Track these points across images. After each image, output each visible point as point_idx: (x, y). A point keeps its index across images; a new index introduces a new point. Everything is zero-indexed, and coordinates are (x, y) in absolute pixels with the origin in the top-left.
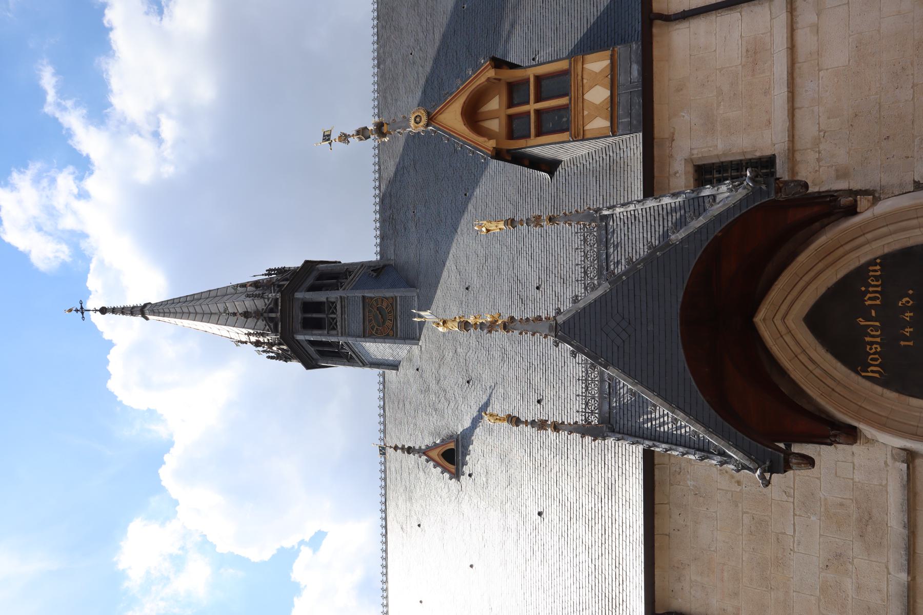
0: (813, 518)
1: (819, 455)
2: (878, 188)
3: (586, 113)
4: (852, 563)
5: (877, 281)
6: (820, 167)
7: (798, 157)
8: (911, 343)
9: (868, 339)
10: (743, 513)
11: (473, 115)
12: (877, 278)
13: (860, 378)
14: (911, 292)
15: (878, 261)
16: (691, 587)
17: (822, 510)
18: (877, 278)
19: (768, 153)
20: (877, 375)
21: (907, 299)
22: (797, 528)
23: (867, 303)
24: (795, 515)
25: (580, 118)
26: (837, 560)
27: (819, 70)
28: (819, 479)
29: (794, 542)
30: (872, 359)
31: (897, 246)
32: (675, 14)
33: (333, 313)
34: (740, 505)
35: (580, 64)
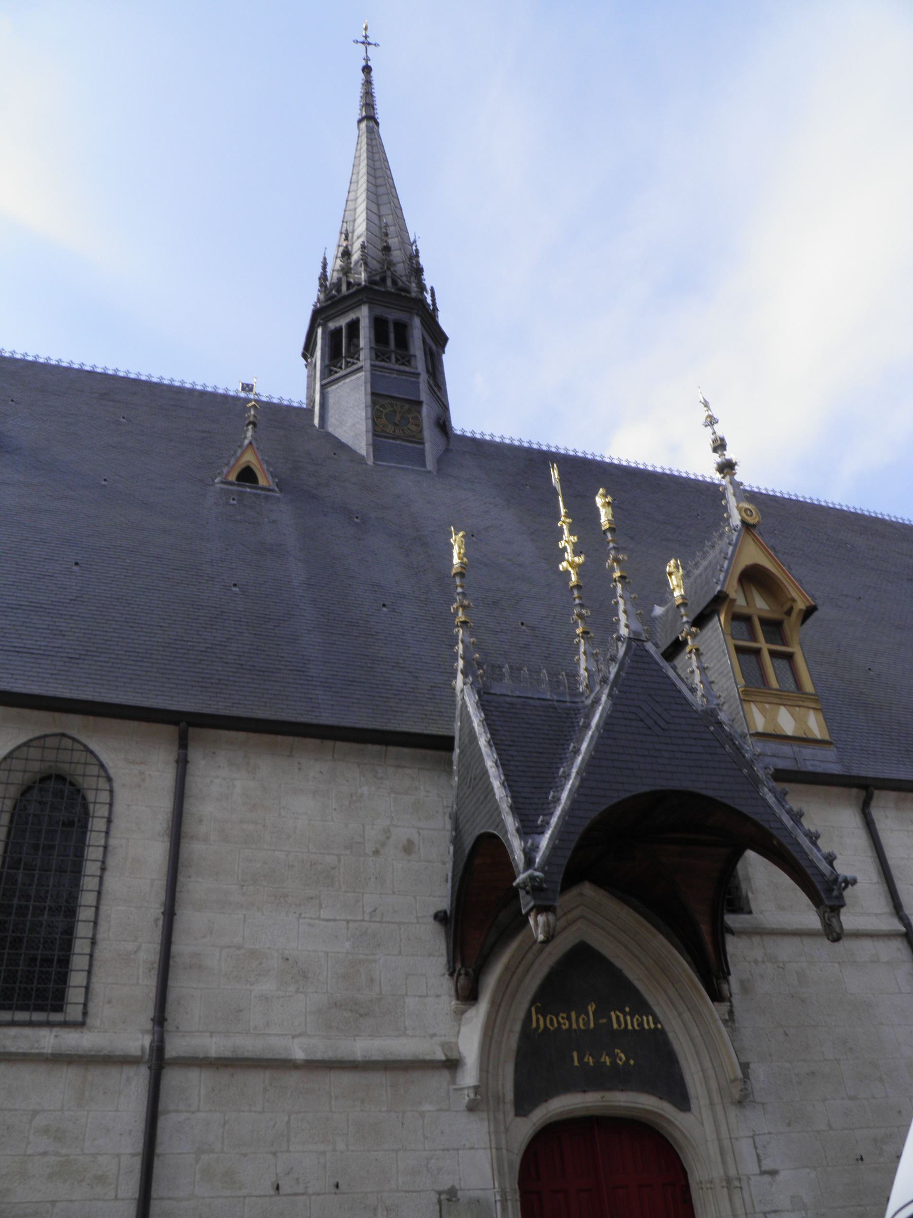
0: (348, 945)
1: (430, 955)
2: (737, 1025)
3: (767, 706)
4: (297, 991)
5: (638, 1025)
6: (749, 963)
7: (756, 939)
8: (576, 1063)
9: (573, 1014)
10: (338, 856)
11: (753, 577)
12: (641, 1024)
13: (525, 1005)
15: (659, 1026)
16: (224, 779)
17: (361, 957)
18: (641, 1024)
19: (753, 906)
20: (534, 1025)
22: (330, 923)
23: (612, 1014)
24: (348, 922)
25: (762, 699)
26: (298, 973)
27: (839, 963)
28: (400, 953)
29: (311, 918)
30: (551, 1020)
31: (676, 1046)
32: (870, 814)
33: (397, 360)
34: (348, 852)
35: (813, 705)
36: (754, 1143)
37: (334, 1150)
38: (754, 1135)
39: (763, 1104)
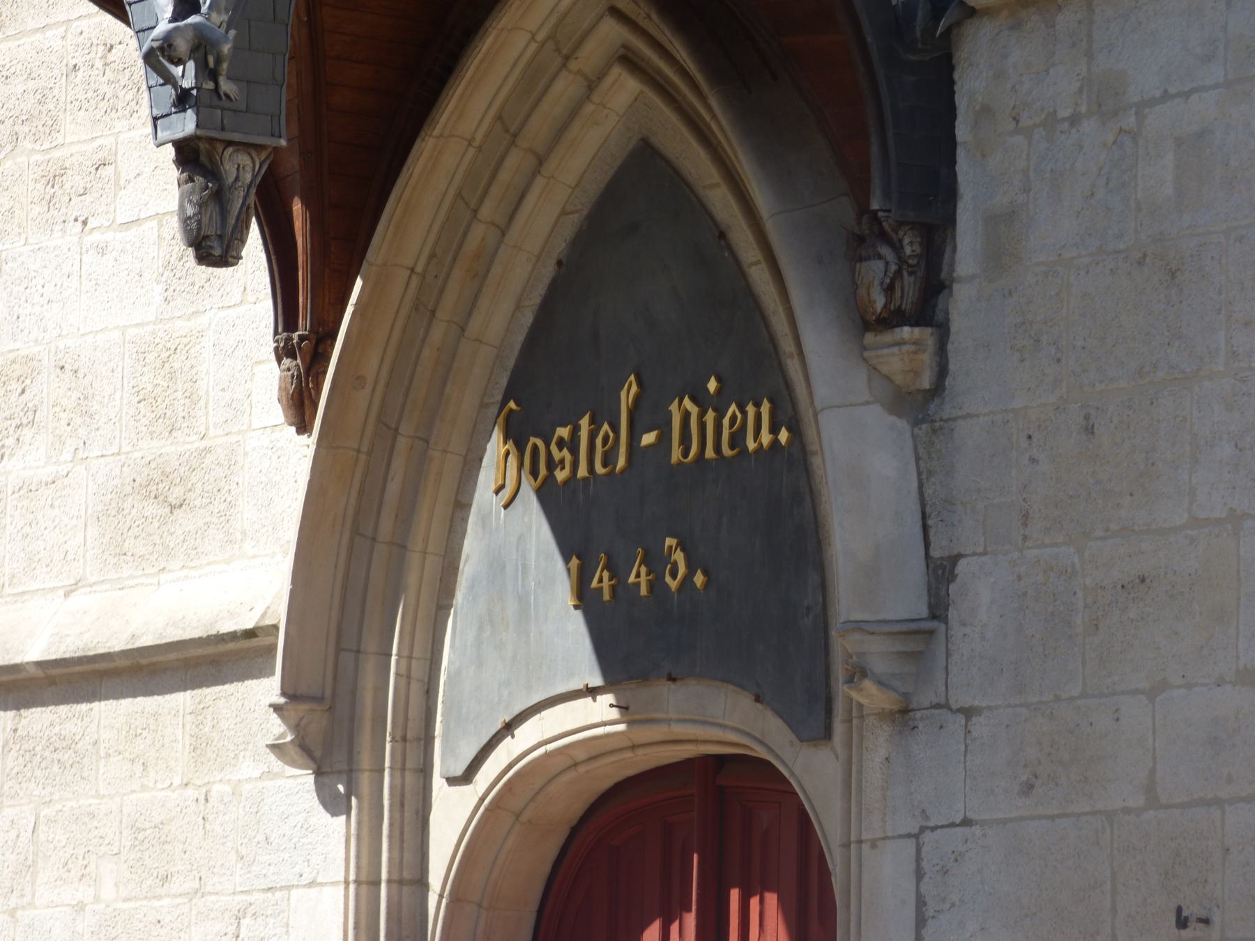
9: (584, 422)
14: (699, 579)
21: (682, 570)
36: (918, 859)
37: (97, 899)
38: (923, 829)
39: (968, 713)
